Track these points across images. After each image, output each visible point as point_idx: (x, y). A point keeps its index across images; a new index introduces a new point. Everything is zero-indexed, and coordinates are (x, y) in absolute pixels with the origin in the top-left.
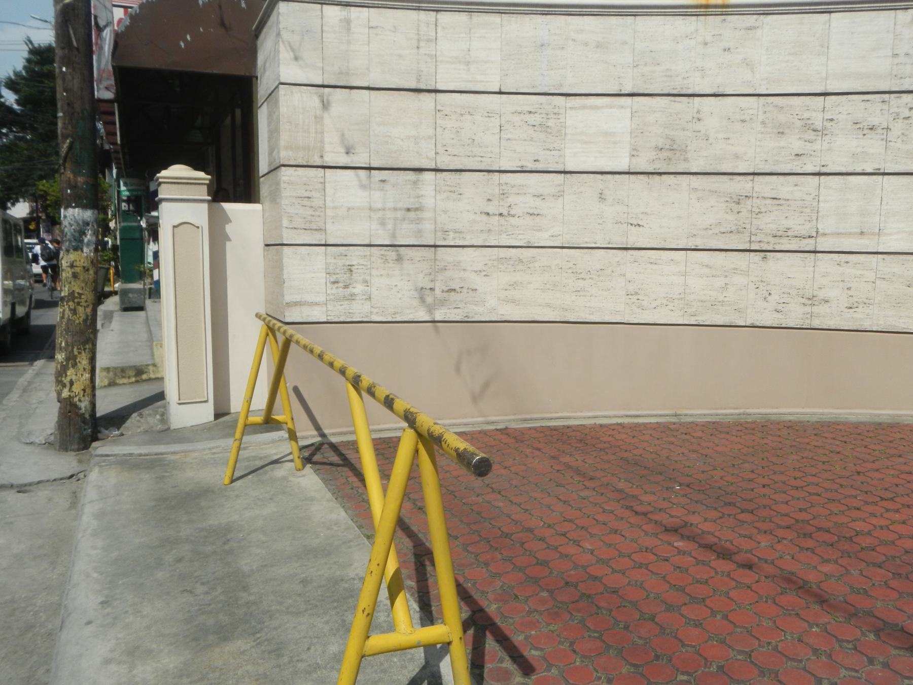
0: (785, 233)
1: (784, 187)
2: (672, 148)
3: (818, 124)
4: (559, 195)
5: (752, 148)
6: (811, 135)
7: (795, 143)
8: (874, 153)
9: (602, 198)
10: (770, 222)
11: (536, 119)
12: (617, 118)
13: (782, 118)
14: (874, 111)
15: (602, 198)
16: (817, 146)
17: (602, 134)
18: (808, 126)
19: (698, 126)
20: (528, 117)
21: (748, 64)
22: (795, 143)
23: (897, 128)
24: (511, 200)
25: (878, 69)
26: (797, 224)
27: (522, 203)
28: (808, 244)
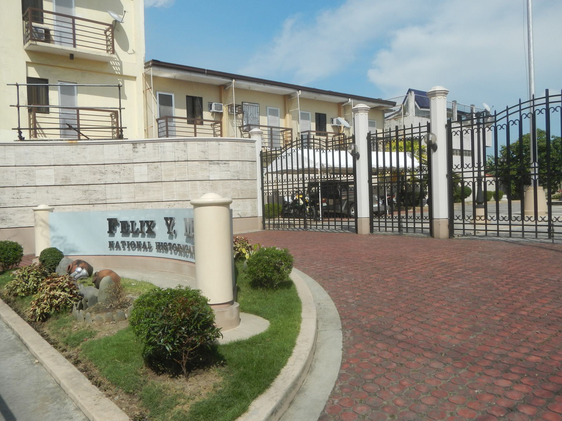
0: (98, 199)
1: (97, 188)
2: (66, 179)
3: (103, 172)
4: (35, 192)
5: (88, 178)
6: (102, 174)
7: (98, 176)
8: (117, 179)
9: (47, 192)
10: (95, 196)
11: (26, 172)
12: (51, 171)
13: (94, 170)
14: (116, 168)
15: (47, 192)
16: (104, 177)
17: (46, 176)
18: (101, 172)
19: (73, 173)
20: (25, 172)
21: (84, 157)
22: (98, 176)
23: (122, 172)
24: (21, 194)
25: (116, 158)
26: (101, 197)
27: (24, 195)
28: (104, 202)
